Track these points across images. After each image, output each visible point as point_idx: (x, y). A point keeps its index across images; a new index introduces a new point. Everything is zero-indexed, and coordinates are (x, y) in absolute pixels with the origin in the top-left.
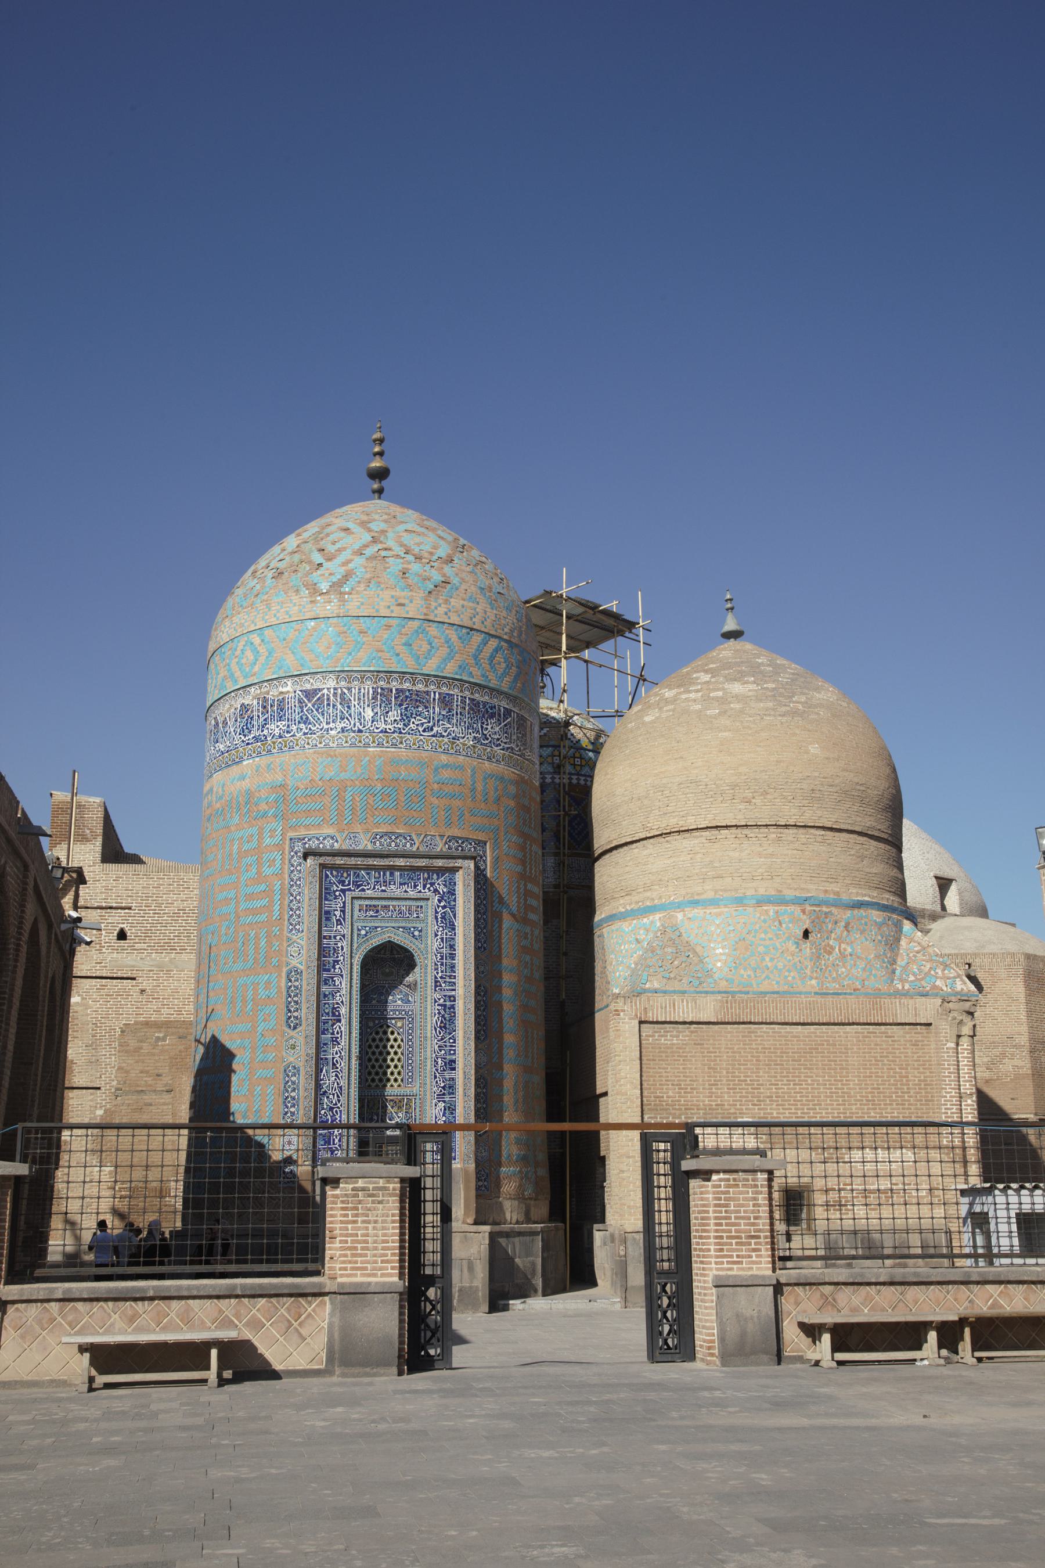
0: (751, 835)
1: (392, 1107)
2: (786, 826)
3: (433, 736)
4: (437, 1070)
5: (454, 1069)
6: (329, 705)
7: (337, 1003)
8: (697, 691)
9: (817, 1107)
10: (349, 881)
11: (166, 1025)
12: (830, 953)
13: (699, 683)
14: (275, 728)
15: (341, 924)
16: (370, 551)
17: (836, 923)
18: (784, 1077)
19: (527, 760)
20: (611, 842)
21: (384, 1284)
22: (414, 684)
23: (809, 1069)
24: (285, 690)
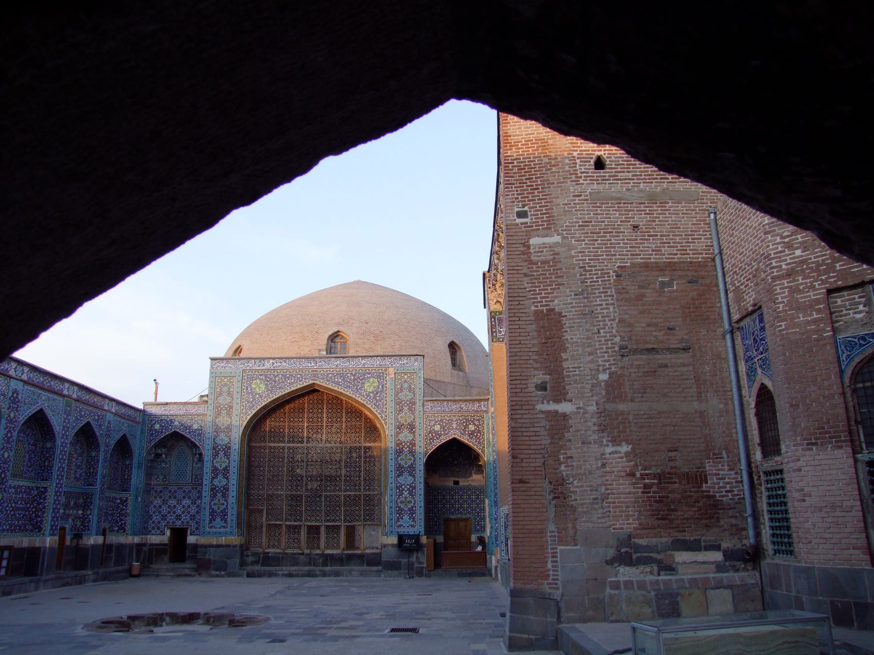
11: (671, 267)
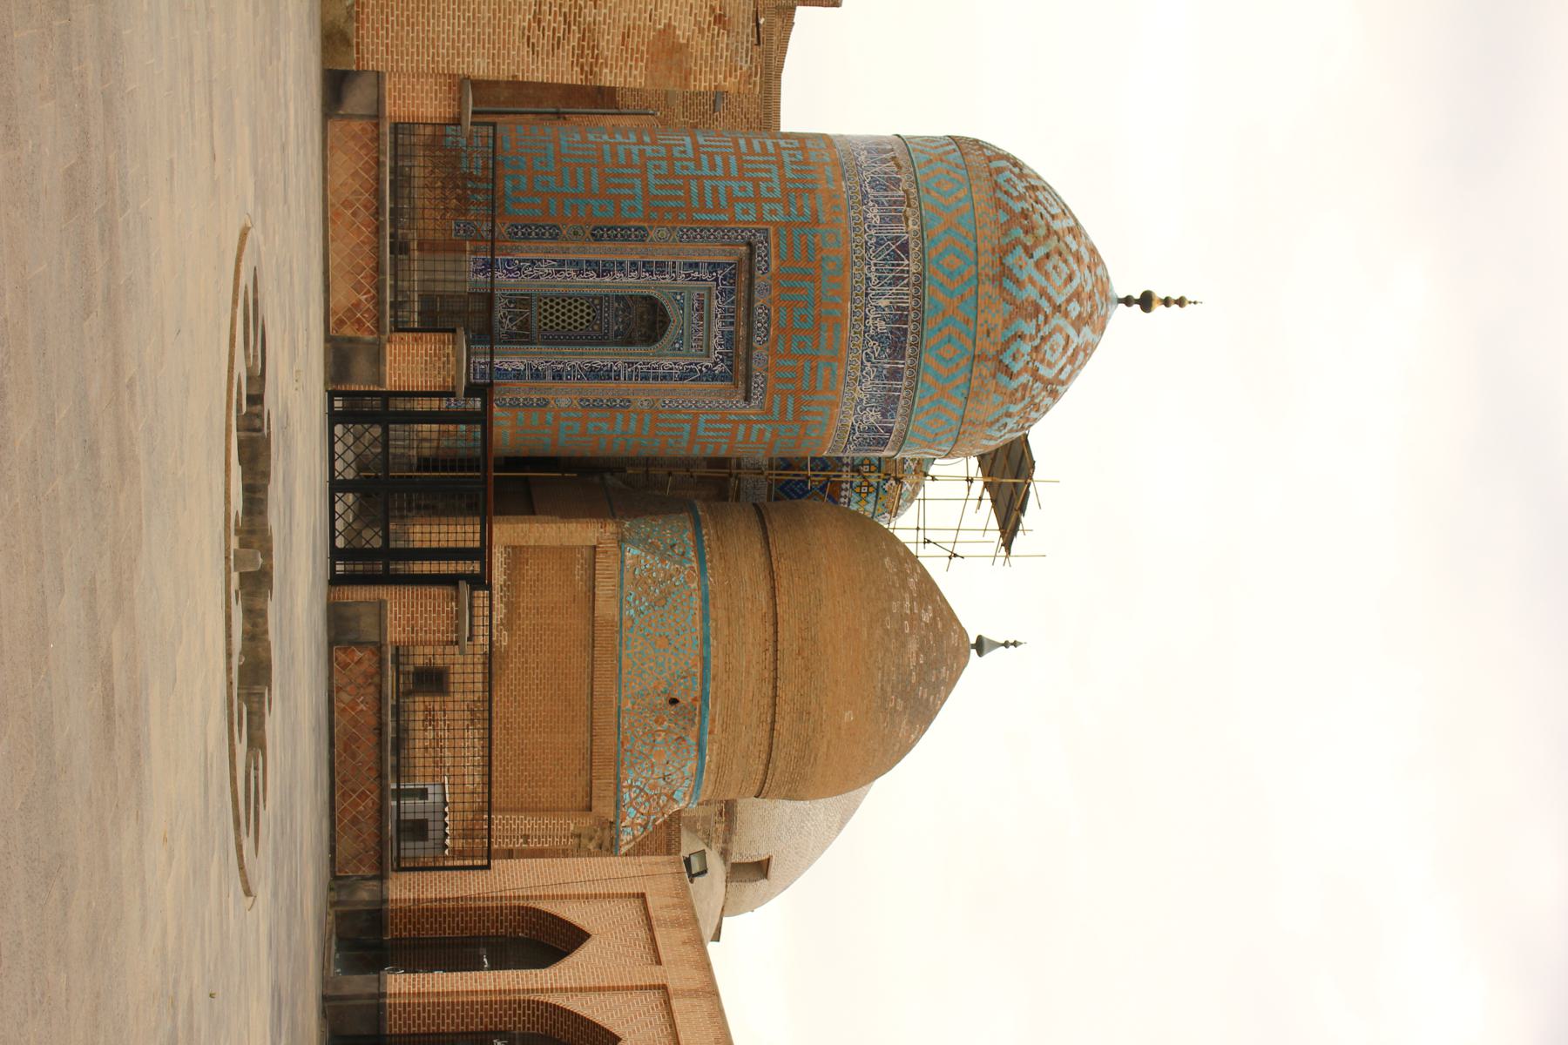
0: (768, 655)
2: (775, 687)
3: (862, 363)
4: (553, 363)
5: (554, 378)
6: (893, 265)
7: (614, 274)
8: (912, 609)
9: (517, 704)
10: (725, 285)
12: (656, 722)
13: (920, 611)
14: (874, 214)
15: (686, 277)
16: (1044, 304)
17: (684, 728)
18: (544, 676)
19: (846, 446)
20: (770, 522)
21: (385, 375)
22: (911, 345)
23: (551, 698)
24: (910, 222)
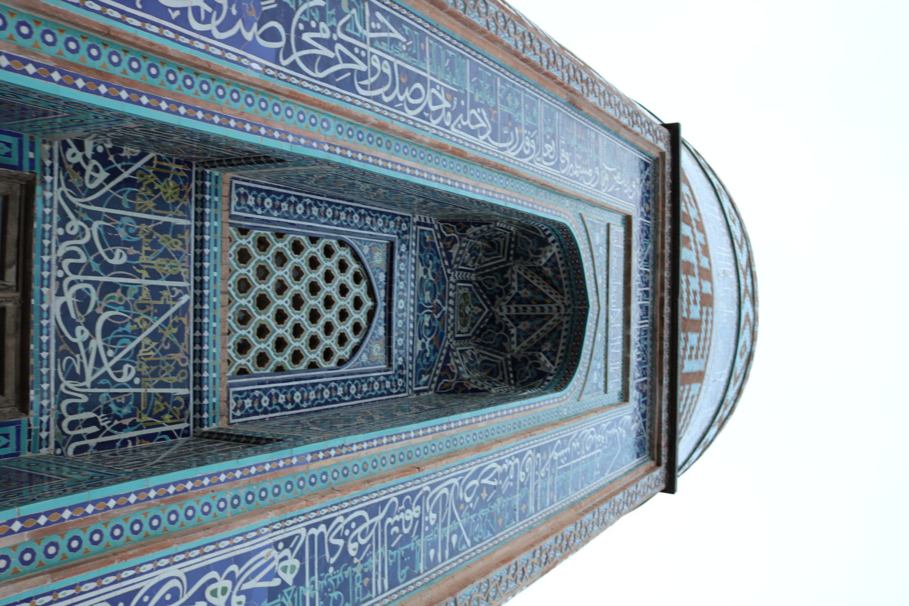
1: (155, 336)
